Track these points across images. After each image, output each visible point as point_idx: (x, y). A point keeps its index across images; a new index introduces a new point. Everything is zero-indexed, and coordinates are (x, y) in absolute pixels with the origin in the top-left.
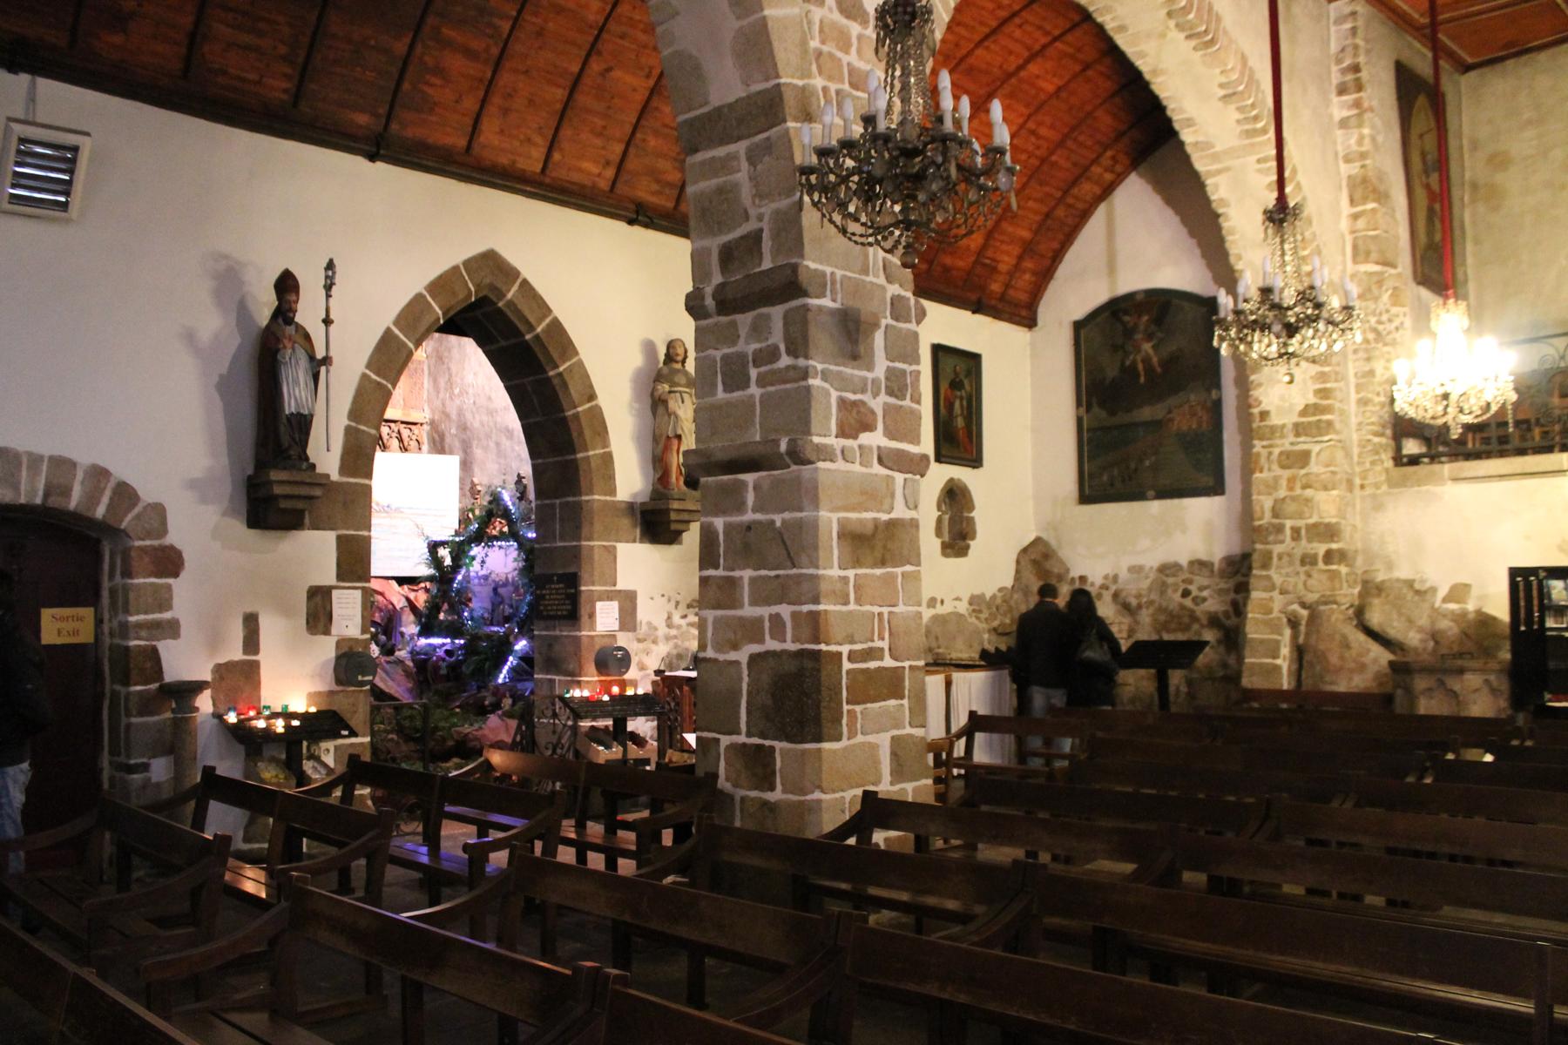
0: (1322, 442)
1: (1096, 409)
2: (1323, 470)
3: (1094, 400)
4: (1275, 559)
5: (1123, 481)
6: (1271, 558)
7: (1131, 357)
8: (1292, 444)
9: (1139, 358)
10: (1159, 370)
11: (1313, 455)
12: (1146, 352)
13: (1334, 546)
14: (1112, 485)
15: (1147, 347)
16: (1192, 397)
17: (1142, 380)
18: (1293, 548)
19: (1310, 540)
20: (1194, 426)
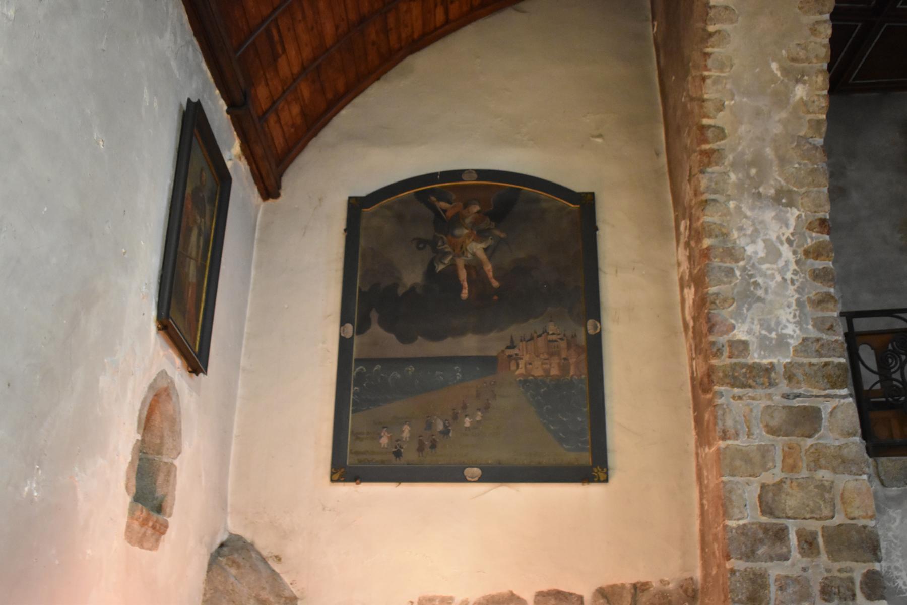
0: (836, 396)
1: (376, 329)
2: (843, 441)
3: (374, 315)
4: (773, 588)
5: (421, 449)
6: (765, 586)
7: (447, 261)
8: (786, 396)
9: (460, 263)
10: (495, 284)
11: (825, 415)
12: (474, 254)
13: (877, 566)
14: (398, 454)
15: (477, 248)
16: (551, 328)
17: (465, 294)
18: (804, 570)
19: (834, 555)
20: (555, 371)
